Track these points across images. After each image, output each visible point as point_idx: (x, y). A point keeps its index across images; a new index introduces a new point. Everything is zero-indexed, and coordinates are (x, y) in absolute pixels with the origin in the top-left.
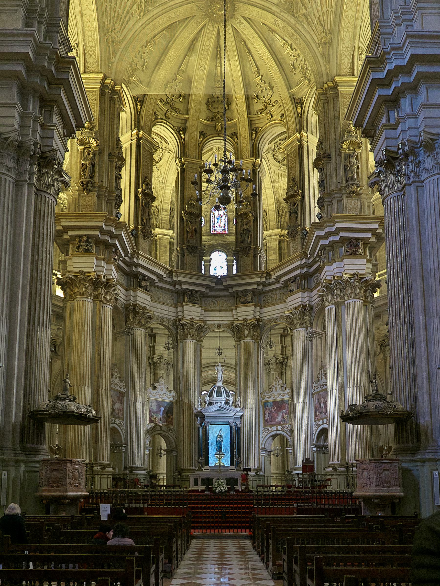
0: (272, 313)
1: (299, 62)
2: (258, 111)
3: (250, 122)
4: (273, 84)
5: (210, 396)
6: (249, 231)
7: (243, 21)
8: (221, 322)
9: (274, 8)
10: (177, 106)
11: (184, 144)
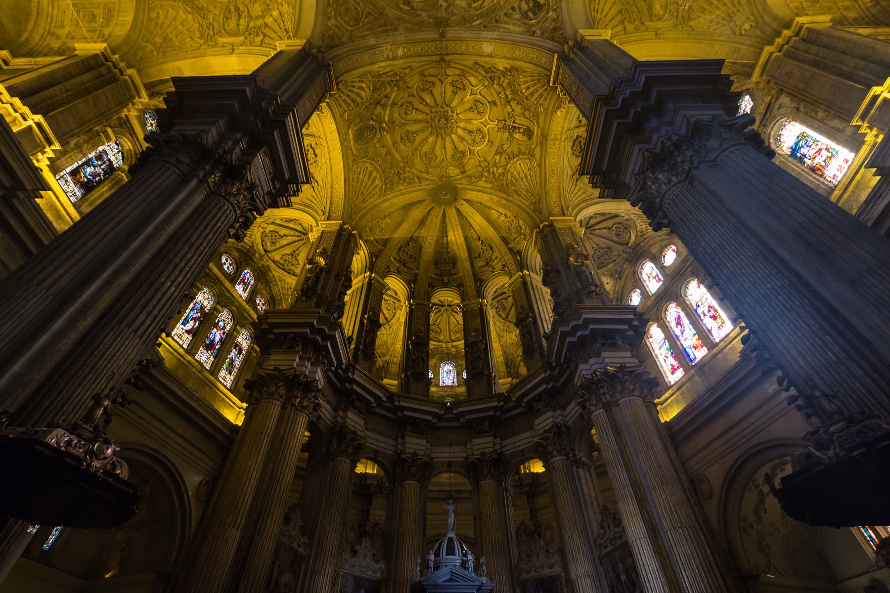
0: (518, 444)
1: (513, 226)
2: (480, 267)
3: (474, 274)
4: (493, 245)
5: (437, 555)
6: (481, 359)
7: (464, 202)
8: (451, 459)
9: (489, 191)
10: (409, 265)
11: (413, 292)
